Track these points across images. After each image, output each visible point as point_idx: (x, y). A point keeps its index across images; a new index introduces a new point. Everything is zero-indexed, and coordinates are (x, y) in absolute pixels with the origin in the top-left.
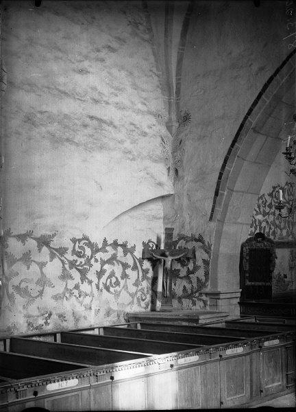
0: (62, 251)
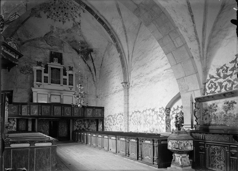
0: (157, 112)
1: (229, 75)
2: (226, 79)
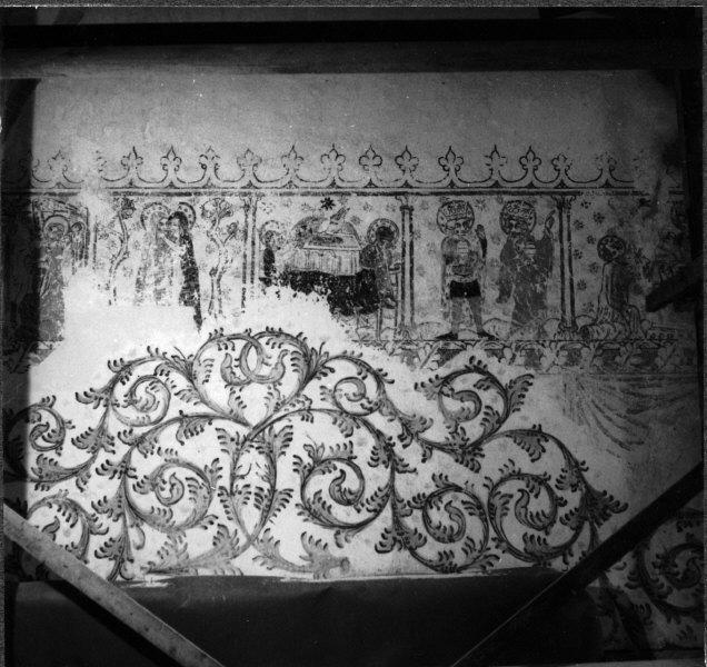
1: (74, 472)
2: (55, 489)
